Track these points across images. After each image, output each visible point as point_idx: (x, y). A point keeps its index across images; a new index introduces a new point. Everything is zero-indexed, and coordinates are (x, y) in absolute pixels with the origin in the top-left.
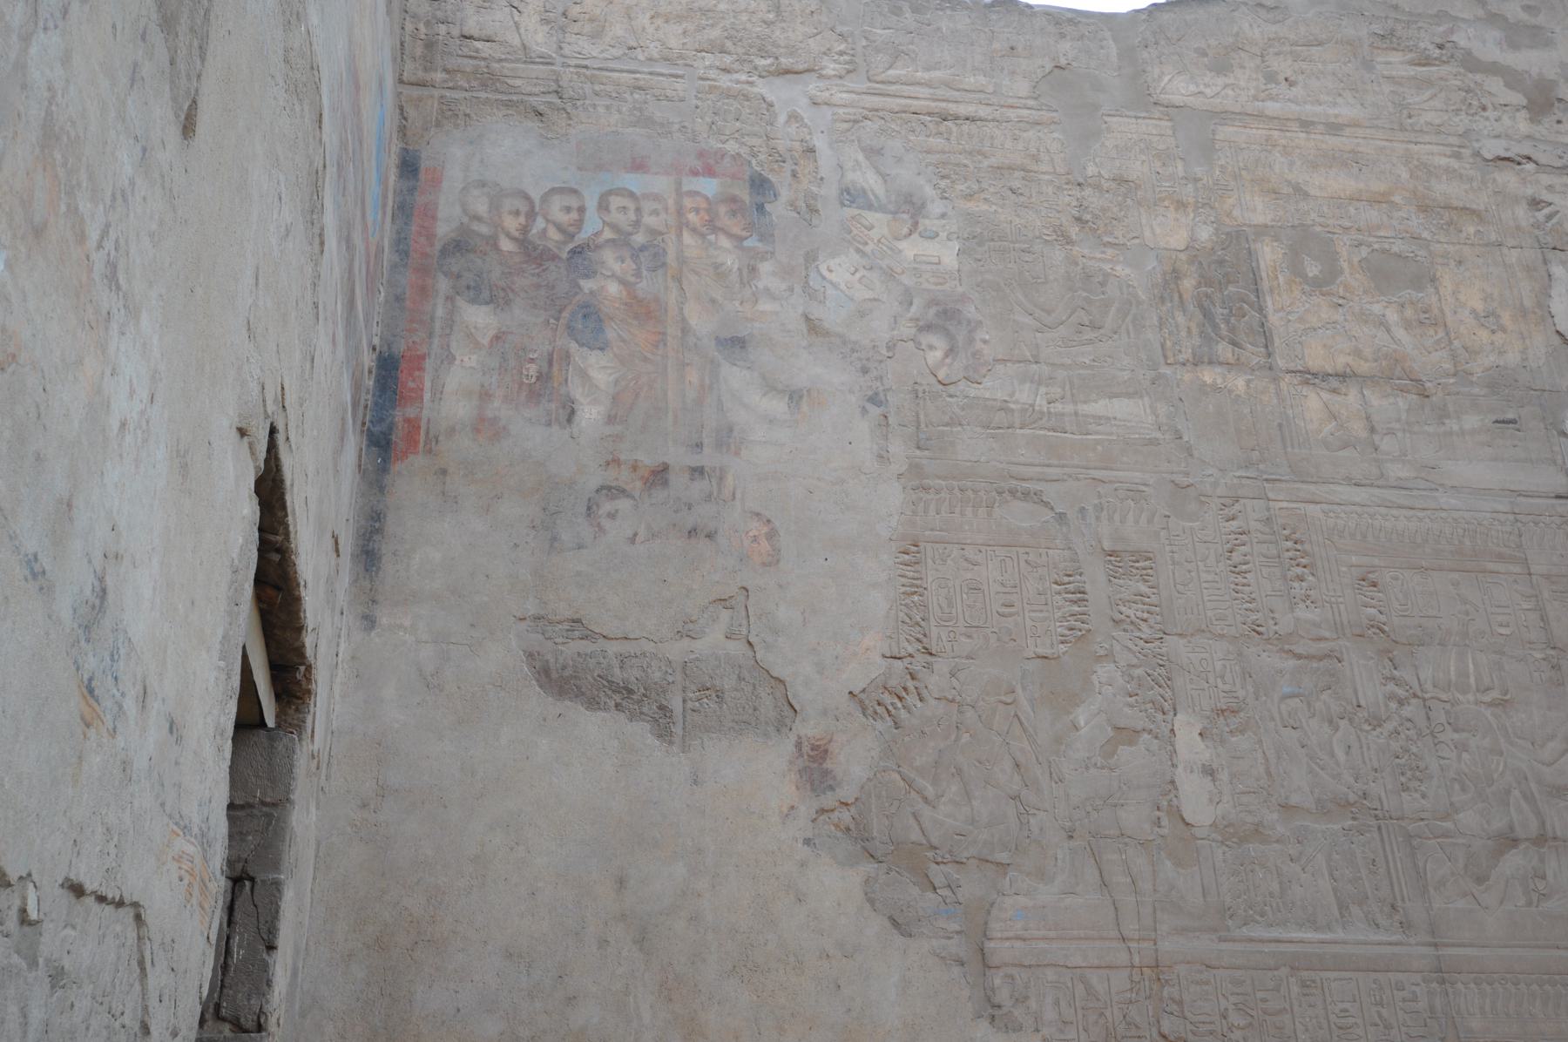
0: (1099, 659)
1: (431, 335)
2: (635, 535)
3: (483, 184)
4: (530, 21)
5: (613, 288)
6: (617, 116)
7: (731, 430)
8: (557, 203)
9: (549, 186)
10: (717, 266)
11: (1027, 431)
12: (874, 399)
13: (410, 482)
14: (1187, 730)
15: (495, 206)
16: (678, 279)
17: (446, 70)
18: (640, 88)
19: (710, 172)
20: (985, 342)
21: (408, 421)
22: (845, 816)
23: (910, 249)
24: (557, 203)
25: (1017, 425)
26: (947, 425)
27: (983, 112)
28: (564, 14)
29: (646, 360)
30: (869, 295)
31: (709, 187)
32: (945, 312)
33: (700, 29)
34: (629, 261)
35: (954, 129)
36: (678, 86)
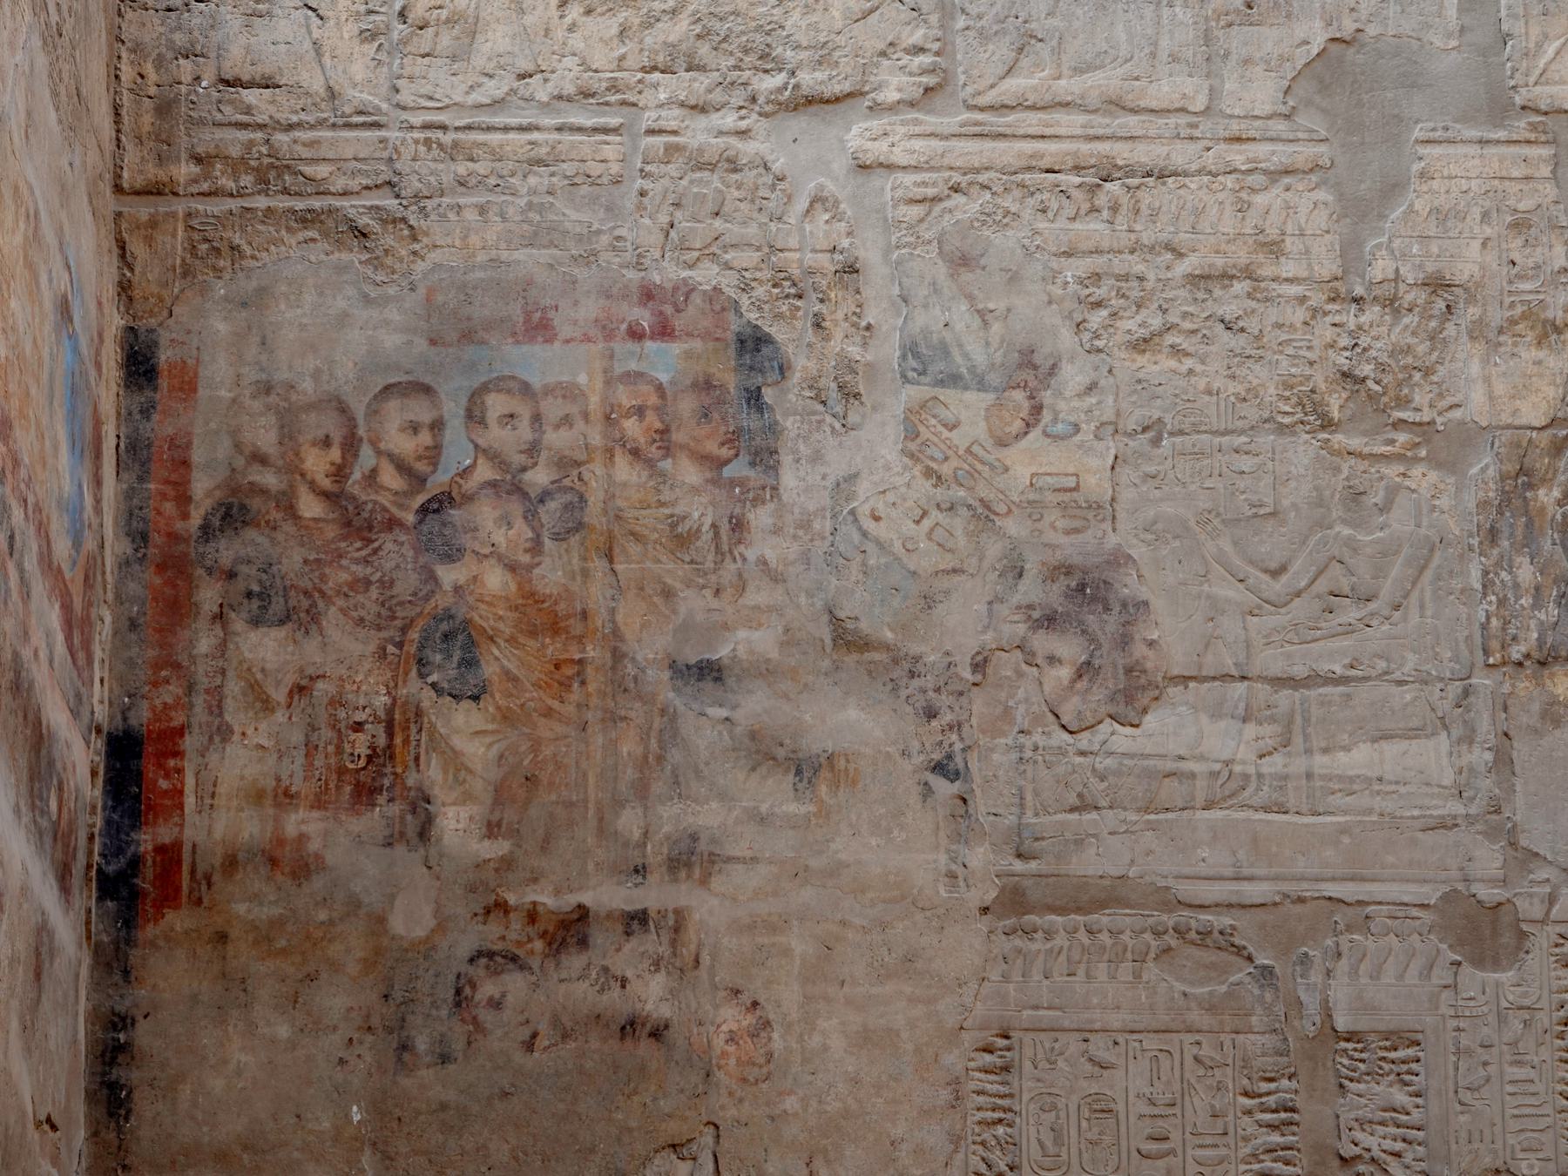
1: (190, 689)
2: (534, 1035)
4: (341, 34)
5: (495, 580)
6: (500, 227)
7: (694, 838)
8: (396, 412)
10: (675, 522)
15: (288, 435)
17: (198, 160)
18: (540, 162)
19: (664, 331)
20: (1151, 644)
21: (160, 849)
23: (1027, 463)
25: (1200, 800)
26: (1072, 810)
27: (1182, 155)
28: (402, 15)
29: (548, 713)
30: (948, 562)
31: (664, 362)
32: (1081, 588)
33: (650, 22)
35: (1125, 200)
36: (609, 152)
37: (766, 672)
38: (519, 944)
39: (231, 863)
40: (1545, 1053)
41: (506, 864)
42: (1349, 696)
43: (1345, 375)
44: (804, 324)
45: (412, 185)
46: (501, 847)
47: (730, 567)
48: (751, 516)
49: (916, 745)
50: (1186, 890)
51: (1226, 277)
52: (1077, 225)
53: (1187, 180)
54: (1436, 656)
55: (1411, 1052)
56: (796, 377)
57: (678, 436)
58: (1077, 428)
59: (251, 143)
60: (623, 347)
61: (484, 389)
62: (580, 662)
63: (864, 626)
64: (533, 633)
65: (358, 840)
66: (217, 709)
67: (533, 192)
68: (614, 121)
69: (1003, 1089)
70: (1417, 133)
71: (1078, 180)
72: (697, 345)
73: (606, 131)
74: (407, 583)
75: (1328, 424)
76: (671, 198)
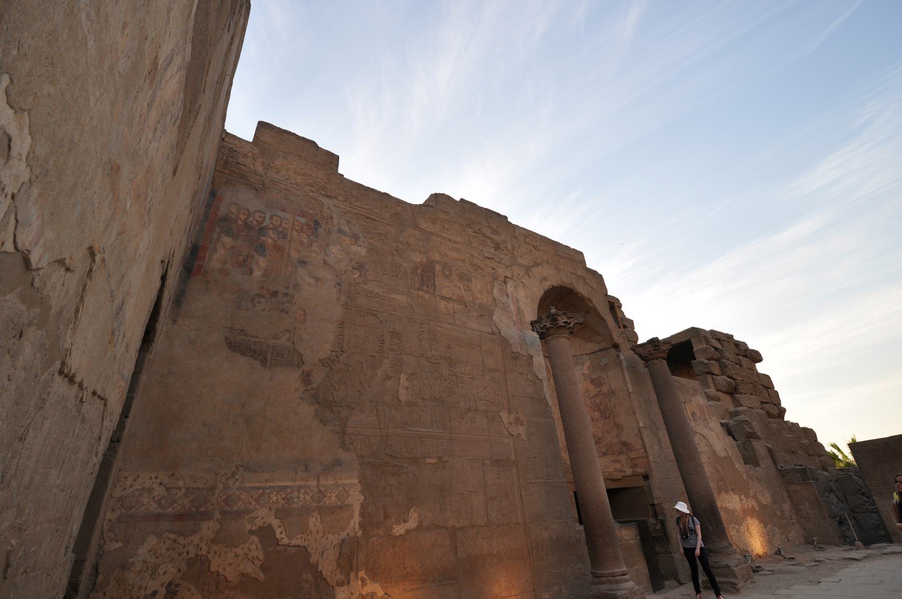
3: (235, 204)
5: (270, 241)
8: (257, 214)
12: (338, 284)
14: (403, 377)
16: (290, 242)
19: (303, 216)
22: (313, 392)
23: (354, 248)
24: (257, 214)
31: (303, 220)
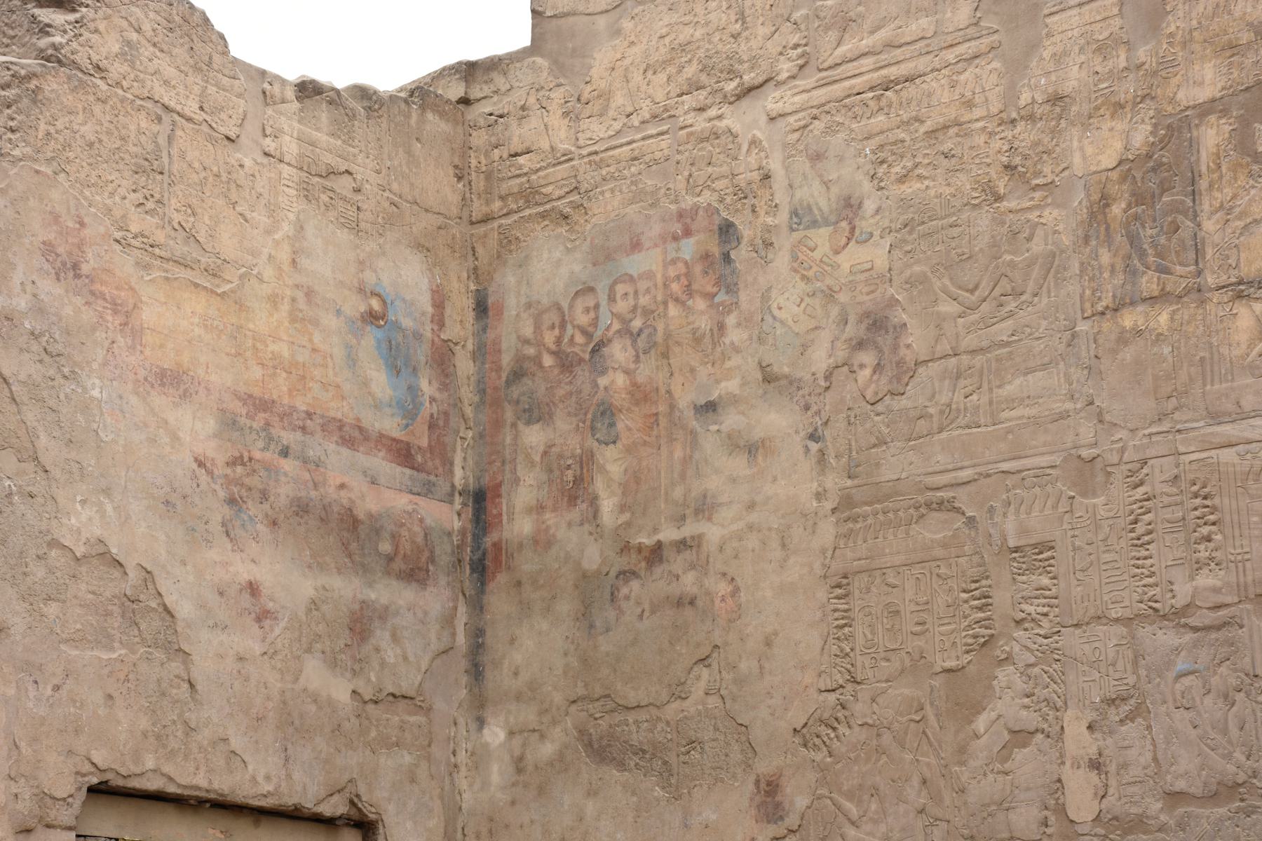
0: (1001, 662)
1: (503, 462)
5: (621, 380)
7: (705, 496)
8: (580, 305)
9: (574, 290)
10: (694, 331)
11: (944, 435)
12: (813, 437)
13: (499, 601)
15: (537, 327)
17: (502, 198)
18: (635, 159)
19: (688, 233)
20: (908, 346)
21: (495, 545)
23: (854, 256)
26: (874, 446)
27: (922, 64)
29: (645, 443)
30: (813, 324)
31: (688, 249)
33: (681, 69)
34: (630, 349)
36: (664, 145)
37: (734, 400)
38: (636, 565)
39: (521, 545)
40: (1123, 543)
41: (628, 524)
42: (1011, 353)
43: (1006, 167)
44: (748, 211)
45: (584, 187)
46: (626, 517)
47: (719, 349)
48: (727, 321)
49: (801, 426)
50: (931, 480)
51: (946, 127)
52: (872, 120)
53: (925, 78)
54: (1057, 319)
55: (1049, 554)
56: (745, 241)
57: (695, 287)
58: (871, 235)
59: (522, 184)
60: (671, 246)
61: (615, 282)
62: (657, 414)
63: (775, 369)
64: (637, 403)
65: (570, 525)
66: (514, 471)
67: (633, 176)
68: (665, 128)
69: (846, 607)
70: (1046, 12)
71: (871, 95)
72: (701, 236)
73: (662, 134)
74: (587, 389)
75: (999, 198)
76: (690, 161)
